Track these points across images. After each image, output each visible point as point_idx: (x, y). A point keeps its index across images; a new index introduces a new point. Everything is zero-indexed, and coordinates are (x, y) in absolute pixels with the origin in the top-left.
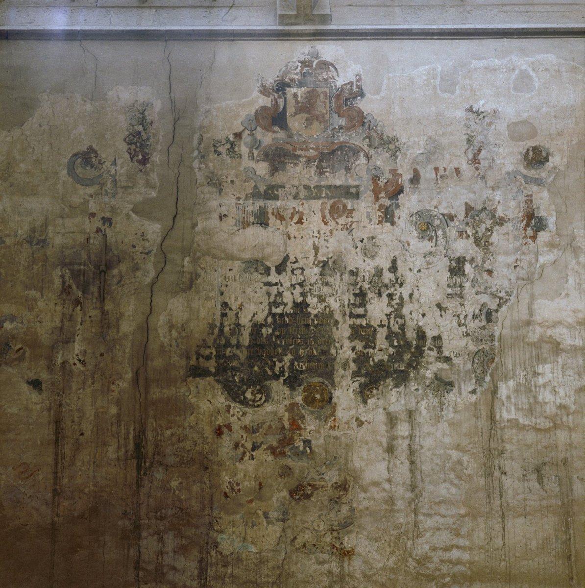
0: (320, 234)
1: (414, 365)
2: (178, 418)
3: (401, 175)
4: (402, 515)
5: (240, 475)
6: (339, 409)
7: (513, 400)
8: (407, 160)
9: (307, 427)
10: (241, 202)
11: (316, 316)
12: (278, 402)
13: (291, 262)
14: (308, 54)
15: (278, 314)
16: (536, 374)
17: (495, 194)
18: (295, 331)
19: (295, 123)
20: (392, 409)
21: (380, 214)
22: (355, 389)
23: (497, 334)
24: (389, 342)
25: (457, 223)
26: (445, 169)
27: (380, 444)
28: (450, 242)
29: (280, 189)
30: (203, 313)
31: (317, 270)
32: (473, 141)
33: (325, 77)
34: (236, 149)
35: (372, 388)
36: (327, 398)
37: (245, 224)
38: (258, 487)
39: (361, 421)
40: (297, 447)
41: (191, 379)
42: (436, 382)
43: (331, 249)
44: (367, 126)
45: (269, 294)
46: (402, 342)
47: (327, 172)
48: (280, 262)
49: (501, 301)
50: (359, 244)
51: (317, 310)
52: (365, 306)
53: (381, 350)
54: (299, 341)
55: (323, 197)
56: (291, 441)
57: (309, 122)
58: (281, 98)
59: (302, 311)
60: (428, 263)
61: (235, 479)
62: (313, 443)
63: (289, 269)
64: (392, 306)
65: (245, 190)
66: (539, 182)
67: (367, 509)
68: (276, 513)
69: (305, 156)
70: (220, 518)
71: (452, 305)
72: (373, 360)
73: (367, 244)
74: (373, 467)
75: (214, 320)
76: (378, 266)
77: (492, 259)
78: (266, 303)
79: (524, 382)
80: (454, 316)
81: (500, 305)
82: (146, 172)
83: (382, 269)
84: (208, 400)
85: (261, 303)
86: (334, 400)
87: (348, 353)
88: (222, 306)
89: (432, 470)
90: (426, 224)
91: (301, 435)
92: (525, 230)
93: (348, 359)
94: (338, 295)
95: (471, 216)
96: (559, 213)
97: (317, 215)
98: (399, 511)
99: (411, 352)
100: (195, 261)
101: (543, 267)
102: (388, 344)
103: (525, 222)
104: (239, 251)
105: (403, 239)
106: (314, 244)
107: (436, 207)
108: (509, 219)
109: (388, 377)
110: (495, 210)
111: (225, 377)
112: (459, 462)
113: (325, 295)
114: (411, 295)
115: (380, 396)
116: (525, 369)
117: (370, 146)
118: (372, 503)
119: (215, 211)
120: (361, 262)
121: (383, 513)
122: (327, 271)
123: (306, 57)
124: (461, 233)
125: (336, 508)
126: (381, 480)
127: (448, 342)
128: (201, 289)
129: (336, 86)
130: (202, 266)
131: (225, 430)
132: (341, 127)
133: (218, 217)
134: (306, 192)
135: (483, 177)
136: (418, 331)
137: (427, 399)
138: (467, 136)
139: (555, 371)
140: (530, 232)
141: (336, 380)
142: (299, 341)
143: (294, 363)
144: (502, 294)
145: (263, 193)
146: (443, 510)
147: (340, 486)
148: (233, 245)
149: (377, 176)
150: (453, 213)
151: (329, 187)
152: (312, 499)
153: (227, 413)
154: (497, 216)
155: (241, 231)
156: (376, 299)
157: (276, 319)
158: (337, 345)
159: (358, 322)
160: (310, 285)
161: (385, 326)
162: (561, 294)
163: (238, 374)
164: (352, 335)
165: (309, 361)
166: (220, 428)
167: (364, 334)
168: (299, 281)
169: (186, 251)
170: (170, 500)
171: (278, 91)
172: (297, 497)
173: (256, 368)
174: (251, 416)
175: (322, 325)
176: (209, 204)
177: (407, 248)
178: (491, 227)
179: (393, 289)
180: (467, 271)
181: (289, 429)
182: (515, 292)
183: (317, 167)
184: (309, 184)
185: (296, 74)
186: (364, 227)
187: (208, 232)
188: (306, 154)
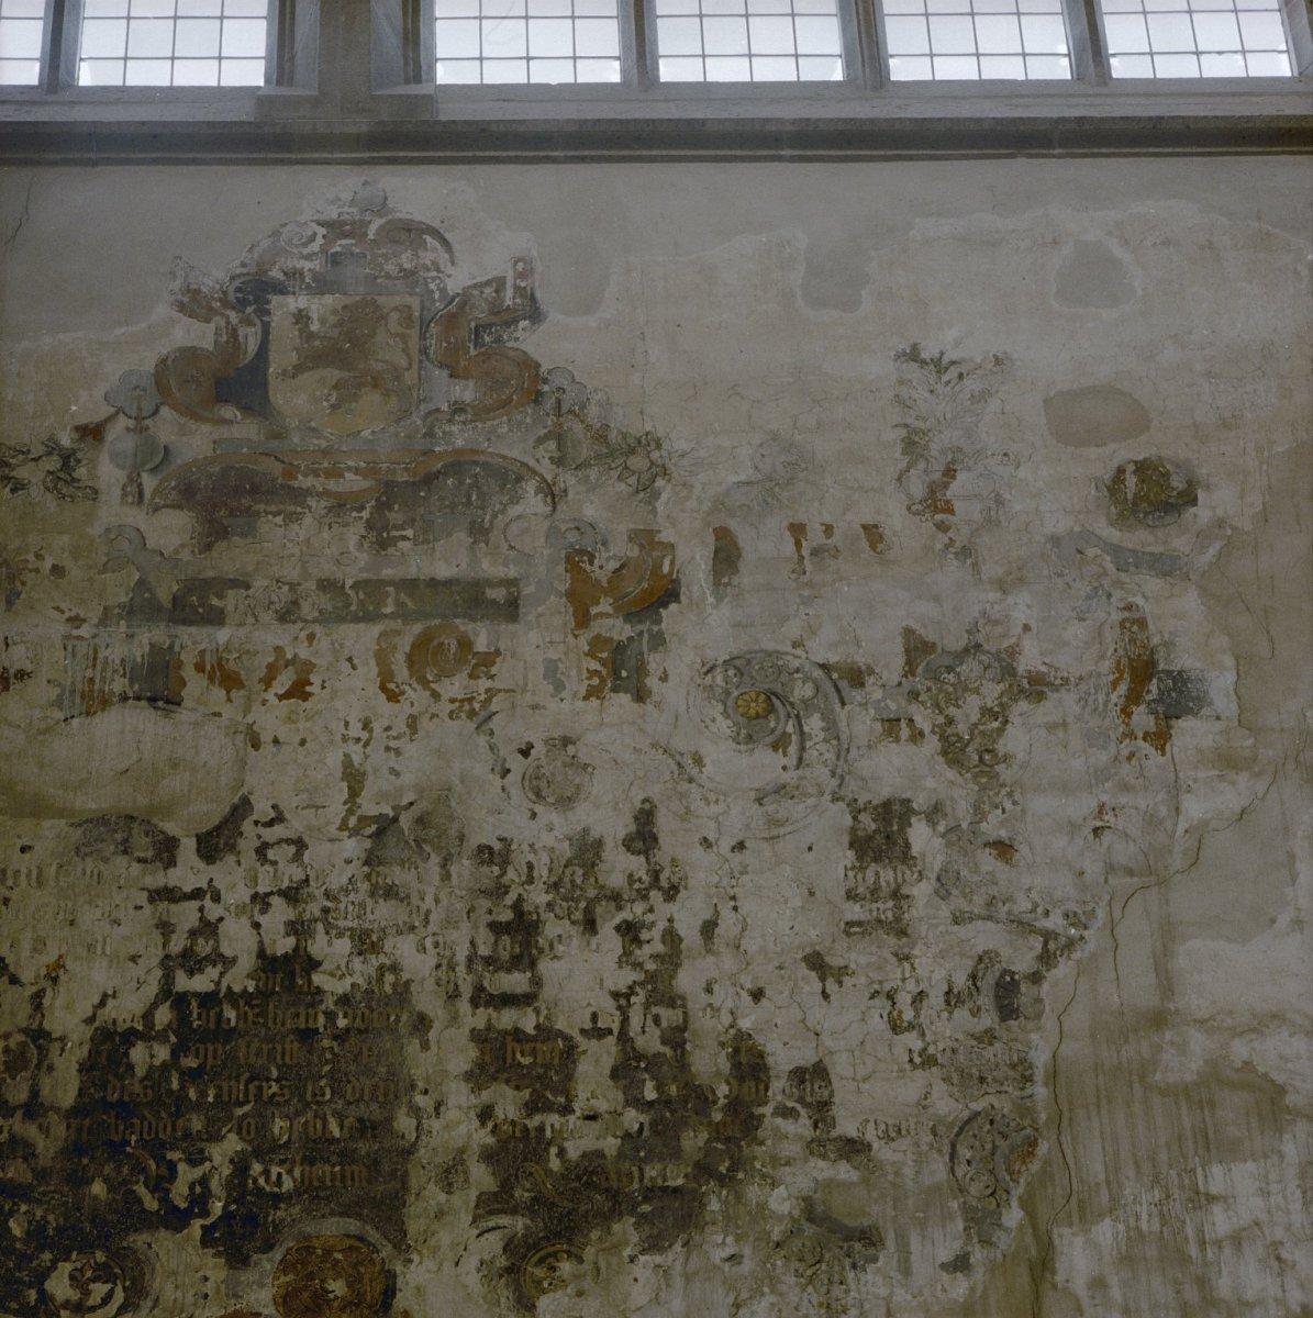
1: (723, 1169)
7: (1116, 1293)
8: (692, 504)
10: (85, 631)
11: (344, 1000)
13: (256, 823)
14: (353, 203)
15: (197, 995)
16: (1201, 1200)
17: (1010, 600)
18: (258, 1054)
19: (298, 399)
21: (595, 665)
22: (487, 1257)
23: (1040, 1059)
24: (626, 1090)
25: (878, 694)
26: (828, 530)
28: (853, 751)
31: (353, 847)
32: (926, 447)
33: (405, 266)
34: (81, 472)
35: (556, 1253)
36: (373, 1291)
37: (93, 701)
42: (809, 1229)
43: (408, 778)
44: (549, 403)
45: (166, 928)
46: (673, 1090)
47: (404, 538)
48: (209, 826)
49: (1052, 946)
50: (517, 764)
51: (348, 981)
52: (533, 965)
53: (592, 1117)
54: (275, 1088)
55: (386, 616)
57: (346, 394)
58: (250, 323)
59: (290, 987)
60: (773, 822)
63: (248, 844)
64: (638, 965)
66: (1166, 566)
69: (327, 493)
71: (863, 960)
72: (562, 1152)
73: (543, 761)
77: (1008, 805)
79: (1156, 1226)
81: (1046, 958)
83: (599, 843)
85: (134, 959)
86: (401, 1301)
87: (463, 1129)
90: (762, 697)
92: (1126, 712)
93: (462, 1151)
94: (432, 928)
95: (926, 670)
96: (1244, 661)
97: (361, 670)
99: (710, 1124)
101: (1199, 832)
102: (621, 1097)
103: (1123, 688)
105: (679, 743)
106: (347, 763)
107: (795, 645)
108: (1066, 681)
109: (621, 1214)
110: (1013, 652)
114: (709, 929)
115: (587, 1284)
116: (1156, 1179)
117: (559, 462)
123: (346, 209)
124: (891, 725)
129: (443, 291)
132: (458, 408)
134: (325, 601)
135: (966, 552)
136: (736, 1051)
138: (903, 432)
139: (1274, 1188)
140: (1142, 718)
141: (414, 1227)
142: (275, 1088)
143: (247, 1168)
144: (1055, 922)
145: (167, 604)
149: (582, 552)
150: (861, 660)
151: (409, 585)
154: (1021, 670)
155: (75, 721)
156: (575, 942)
158: (419, 1099)
159: (507, 1018)
161: (610, 1032)
162: (1273, 921)
163: (24, 1208)
164: (481, 1066)
165: (309, 1161)
167: (526, 1062)
168: (286, 884)
171: (241, 304)
173: (98, 1188)
175: (366, 1030)
177: (694, 771)
178: (1001, 705)
179: (639, 908)
180: (916, 850)
182: (1101, 914)
183: (370, 525)
184: (339, 575)
185: (308, 257)
186: (535, 707)
188: (332, 485)
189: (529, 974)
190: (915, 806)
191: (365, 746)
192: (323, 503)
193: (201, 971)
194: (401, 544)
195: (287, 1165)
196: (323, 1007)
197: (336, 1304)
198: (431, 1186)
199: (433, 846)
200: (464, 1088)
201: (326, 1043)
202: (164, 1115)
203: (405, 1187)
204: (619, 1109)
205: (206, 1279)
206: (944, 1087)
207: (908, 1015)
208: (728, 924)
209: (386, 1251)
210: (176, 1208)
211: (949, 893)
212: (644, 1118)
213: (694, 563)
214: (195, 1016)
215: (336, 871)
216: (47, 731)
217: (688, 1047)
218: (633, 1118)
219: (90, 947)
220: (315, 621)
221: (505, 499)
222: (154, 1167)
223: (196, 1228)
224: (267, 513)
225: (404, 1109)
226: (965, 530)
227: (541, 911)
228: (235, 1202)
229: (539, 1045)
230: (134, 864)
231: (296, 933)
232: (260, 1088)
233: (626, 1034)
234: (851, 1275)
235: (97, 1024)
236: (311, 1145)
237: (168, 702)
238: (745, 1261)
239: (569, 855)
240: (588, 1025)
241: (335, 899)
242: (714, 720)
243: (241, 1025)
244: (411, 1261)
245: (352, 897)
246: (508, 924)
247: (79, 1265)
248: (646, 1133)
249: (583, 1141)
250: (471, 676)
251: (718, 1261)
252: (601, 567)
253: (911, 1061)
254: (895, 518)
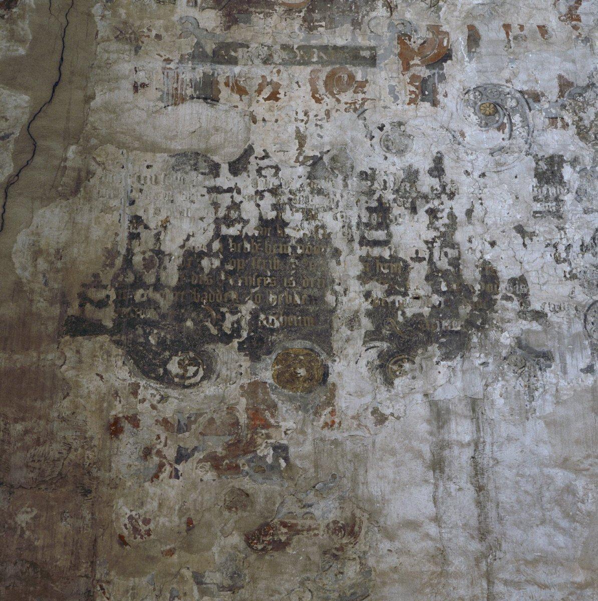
0: (308, 116)
1: (478, 323)
2: (38, 404)
3: (447, 33)
4: (464, 582)
5: (152, 506)
6: (341, 393)
8: (456, 14)
9: (281, 424)
10: (172, 66)
11: (300, 241)
12: (228, 380)
13: (256, 158)
15: (231, 236)
18: (261, 264)
20: (439, 395)
24: (432, 286)
25: (547, 106)
26: (522, 28)
27: (419, 455)
28: (536, 132)
29: (240, 50)
30: (96, 233)
31: (301, 170)
35: (402, 360)
36: (318, 374)
37: (178, 99)
38: (184, 526)
39: (383, 415)
40: (261, 458)
41: (67, 338)
42: (519, 352)
43: (326, 139)
45: (216, 205)
46: (454, 286)
47: (321, 26)
48: (234, 158)
50: (377, 133)
51: (302, 232)
52: (387, 227)
53: (417, 298)
54: (269, 280)
55: (313, 63)
56: (250, 447)
59: (275, 234)
61: (141, 511)
62: (292, 450)
65: (179, 48)
67: (395, 569)
68: (218, 575)
70: (108, 582)
71: (542, 229)
72: (403, 313)
73: (390, 133)
74: (406, 496)
75: (115, 244)
76: (410, 166)
78: (211, 218)
80: (547, 246)
82: (10, 18)
84: (97, 375)
85: (202, 219)
86: (331, 379)
87: (357, 301)
88: (131, 222)
89: (519, 502)
90: (492, 106)
91: (268, 437)
93: (357, 312)
94: (340, 209)
95: (570, 94)
97: (303, 88)
98: (458, 575)
99: (472, 302)
100: (87, 152)
104: (166, 138)
105: (453, 126)
106: (298, 131)
107: (507, 81)
109: (432, 343)
111: (131, 336)
112: (569, 489)
113: (317, 209)
114: (469, 213)
115: (417, 374)
118: (404, 559)
119: (126, 77)
120: (380, 159)
121: (426, 578)
122: (320, 172)
124: (553, 120)
125: (336, 566)
126: (421, 519)
127: (538, 286)
128: (95, 195)
130: (98, 159)
131: (127, 426)
133: (131, 87)
134: (284, 55)
136: (484, 269)
137: (503, 379)
142: (269, 280)
143: (258, 316)
146: (541, 574)
147: (343, 527)
148: (155, 128)
149: (405, 35)
150: (539, 89)
151: (324, 48)
152: (289, 550)
153: (131, 396)
155: (170, 108)
156: (407, 217)
157: (228, 245)
158: (337, 288)
159: (376, 252)
160: (290, 192)
161: (424, 259)
163: (155, 331)
164: (364, 273)
165: (286, 314)
166: (117, 420)
167: (385, 271)
168: (271, 186)
169: (71, 136)
170: (14, 547)
172: (260, 547)
173: (189, 323)
174: (176, 403)
175: (311, 255)
176: (116, 67)
177: (461, 140)
180: (566, 178)
181: (248, 426)
183: (304, 20)
184: (291, 43)
186: (385, 107)
187: (107, 108)
189: (386, 232)
190: (565, 158)
191: (306, 124)
192: (282, 9)
193: (233, 225)
194: (319, 29)
195: (277, 316)
196: (290, 244)
197: (301, 379)
198: (344, 327)
199: (339, 171)
200: (357, 283)
201: (292, 260)
202: (218, 291)
203: (331, 327)
204: (430, 294)
205: (241, 366)
206: (581, 288)
207: (564, 255)
208: (478, 211)
209: (324, 356)
210: (226, 334)
211: (582, 200)
212: (441, 299)
213: (459, 41)
214: (231, 246)
215: (294, 181)
216: (157, 112)
217: (461, 267)
218: (436, 299)
219: (181, 213)
220: (280, 64)
221: (368, 9)
222: (215, 314)
223: (235, 343)
224: (256, 12)
225: (330, 292)
226: (586, 29)
227: (391, 202)
228: (253, 332)
229: (391, 264)
230: (200, 175)
231: (277, 210)
232: (263, 280)
233: (432, 260)
234: (539, 373)
235: (185, 248)
236: (287, 307)
237: (213, 100)
238: (490, 365)
239: (403, 177)
240: (414, 256)
241: (294, 194)
242: (469, 116)
243: (253, 251)
244: (335, 361)
245: (302, 193)
246: (376, 208)
247: (182, 358)
248: (442, 306)
249: (412, 309)
250: (355, 92)
251: (477, 365)
252: (414, 42)
253: (565, 276)
254: (553, 22)
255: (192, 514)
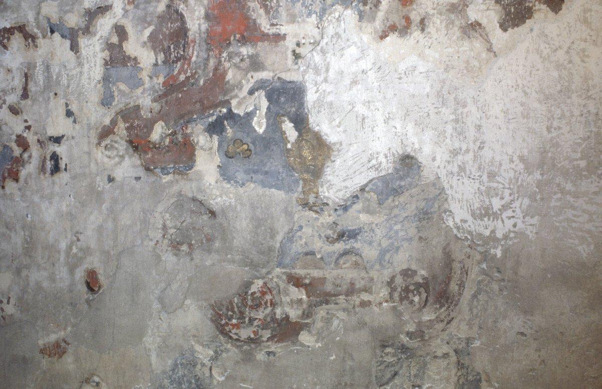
9: (285, 29)
91: (256, 64)
147: (425, 285)
152: (305, 338)
172: (245, 333)
255: (94, 262)
